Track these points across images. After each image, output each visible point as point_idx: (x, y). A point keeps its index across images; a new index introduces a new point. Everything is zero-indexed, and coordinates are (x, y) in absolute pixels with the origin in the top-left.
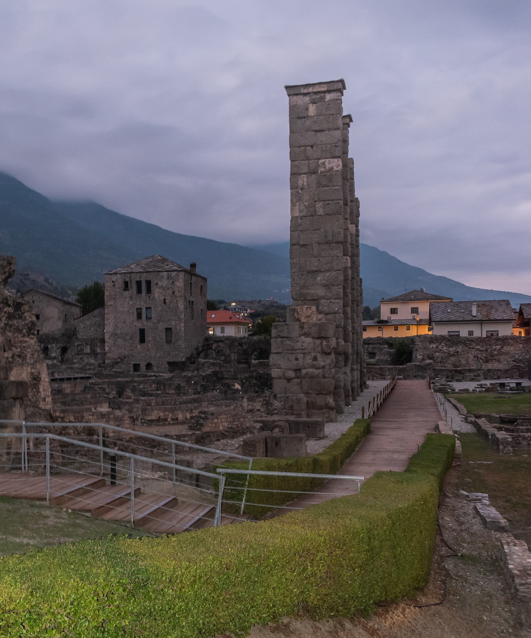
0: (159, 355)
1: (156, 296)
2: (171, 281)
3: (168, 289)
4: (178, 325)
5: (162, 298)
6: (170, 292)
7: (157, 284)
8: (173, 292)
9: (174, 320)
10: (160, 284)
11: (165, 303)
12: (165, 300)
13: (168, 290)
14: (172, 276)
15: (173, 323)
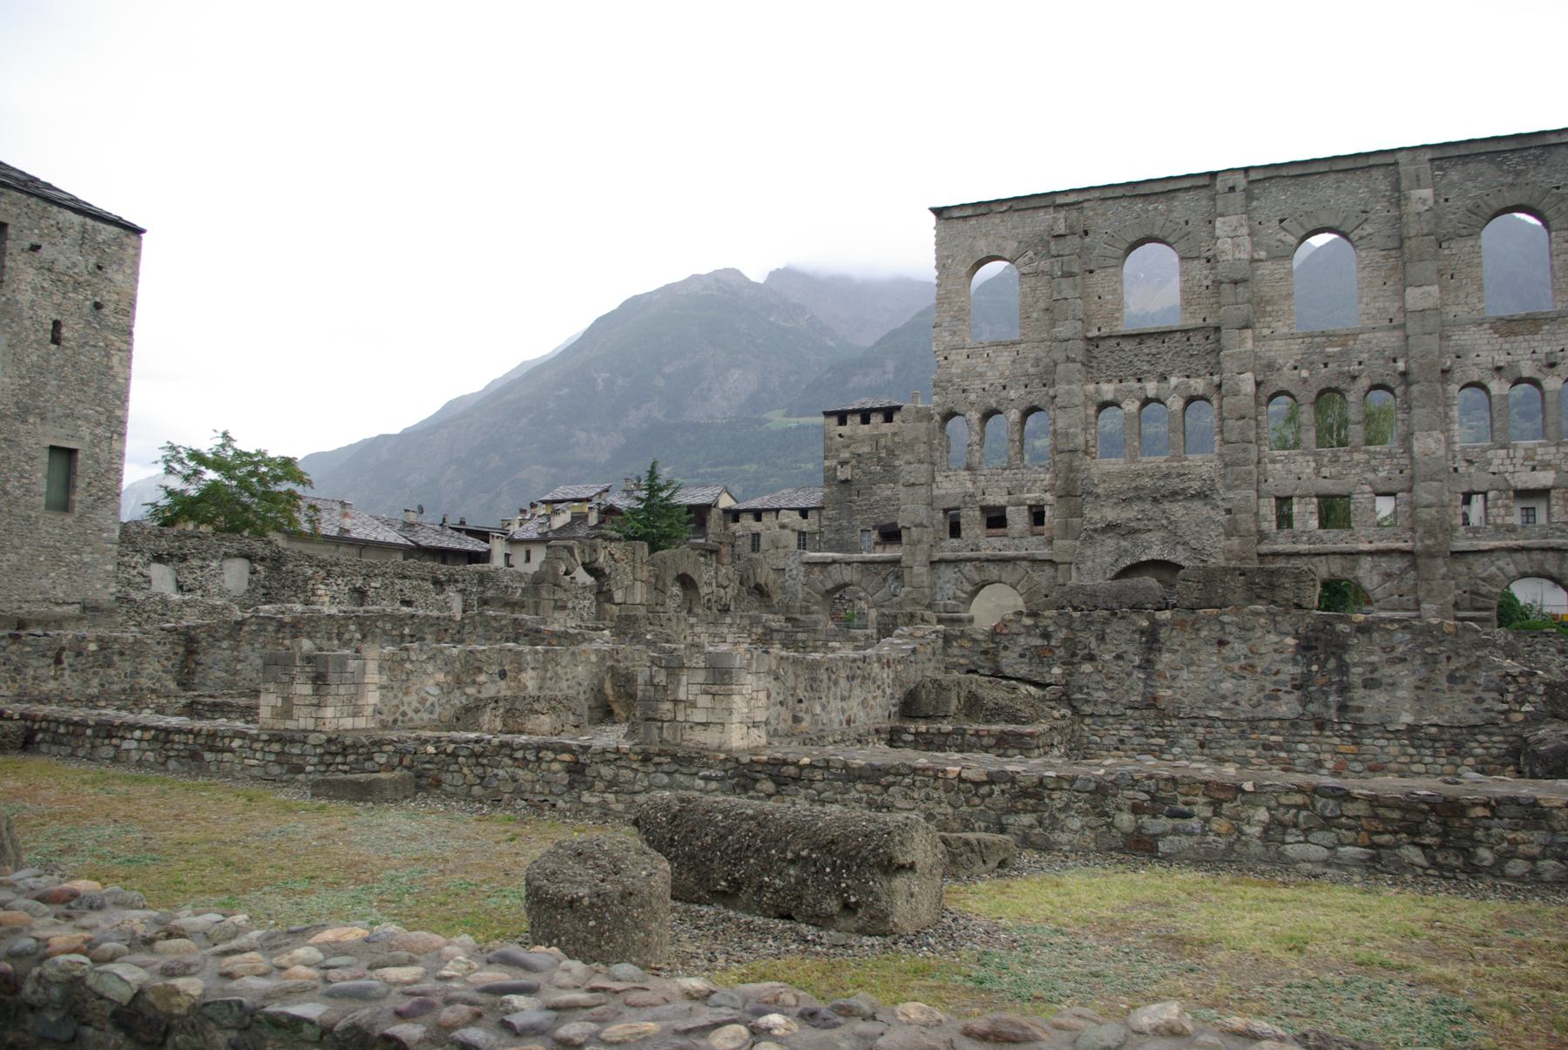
0: (14, 558)
1: (25, 298)
2: (93, 260)
3: (77, 285)
4: (104, 445)
5: (48, 315)
6: (84, 298)
7: (35, 248)
8: (98, 306)
9: (86, 418)
10: (47, 252)
11: (56, 340)
12: (57, 324)
13: (75, 290)
14: (100, 239)
15: (85, 431)
